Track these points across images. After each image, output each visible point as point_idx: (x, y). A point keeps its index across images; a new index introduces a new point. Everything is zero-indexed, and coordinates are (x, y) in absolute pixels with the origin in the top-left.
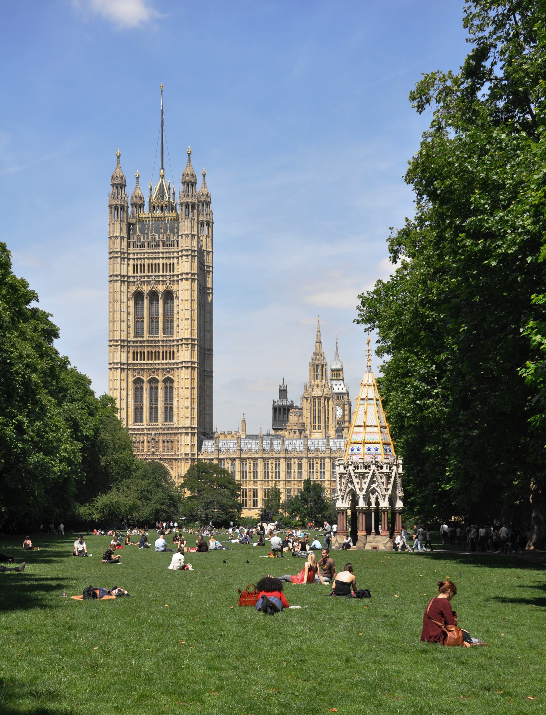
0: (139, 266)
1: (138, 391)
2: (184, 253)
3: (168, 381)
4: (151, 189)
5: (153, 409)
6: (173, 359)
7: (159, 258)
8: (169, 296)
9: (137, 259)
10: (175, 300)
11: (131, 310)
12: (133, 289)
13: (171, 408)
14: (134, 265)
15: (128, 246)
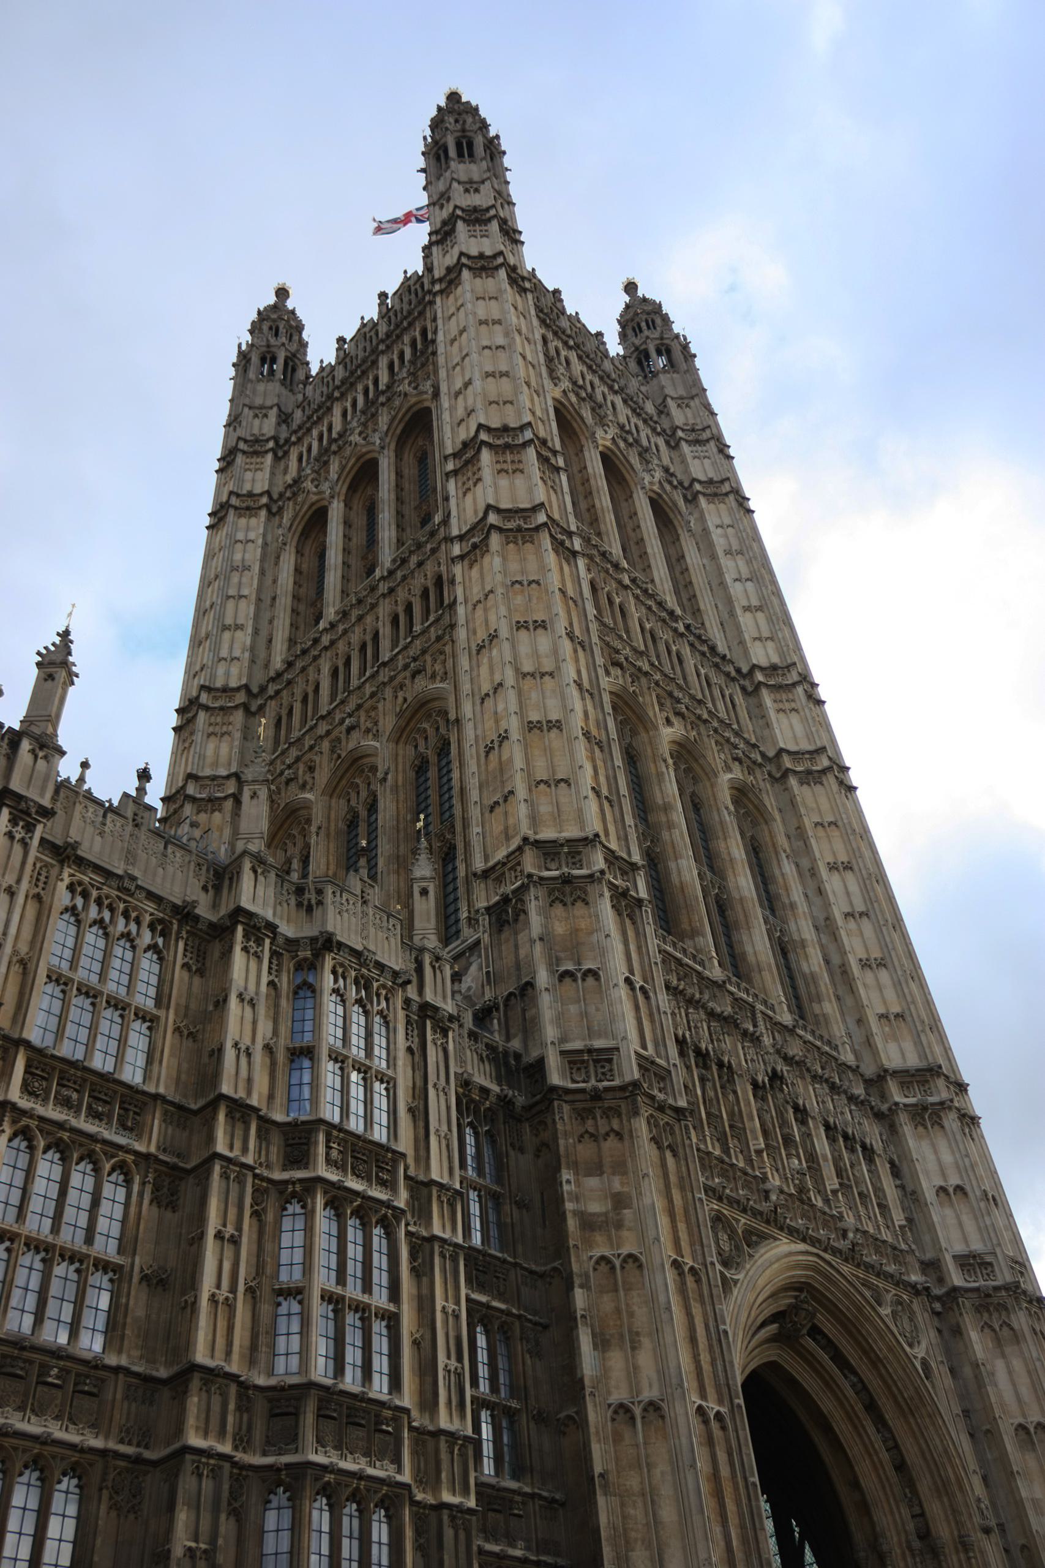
7: (375, 363)
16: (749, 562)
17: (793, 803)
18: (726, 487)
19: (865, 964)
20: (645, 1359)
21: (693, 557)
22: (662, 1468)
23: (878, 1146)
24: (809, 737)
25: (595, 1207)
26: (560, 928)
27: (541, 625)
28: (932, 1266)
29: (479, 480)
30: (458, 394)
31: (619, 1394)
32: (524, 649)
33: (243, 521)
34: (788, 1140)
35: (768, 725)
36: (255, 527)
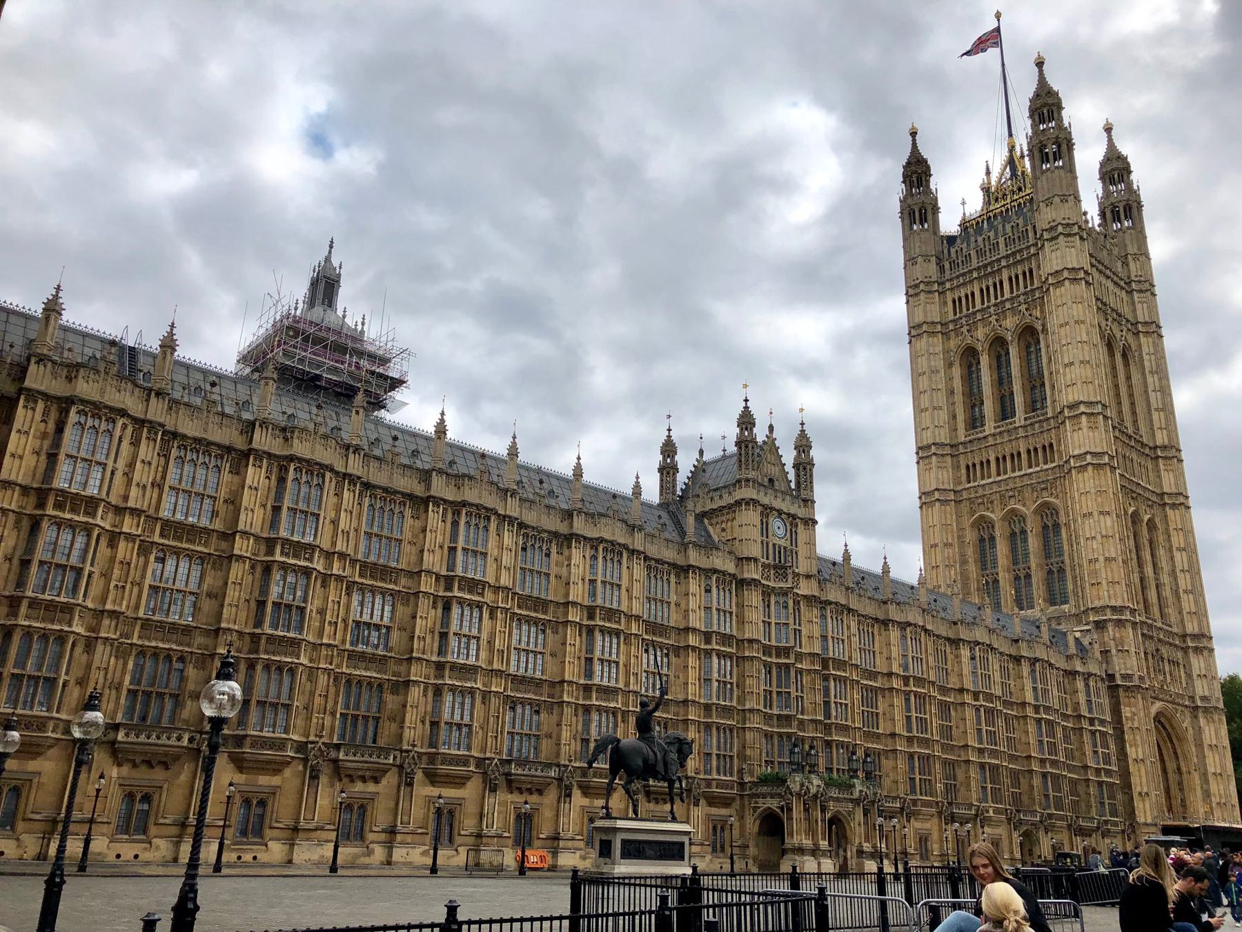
0: (964, 300)
1: (985, 544)
2: (1046, 235)
3: (1046, 510)
4: (988, 173)
5: (1022, 580)
6: (1053, 461)
7: (999, 270)
8: (1030, 335)
9: (958, 286)
10: (1041, 337)
11: (957, 384)
12: (953, 344)
13: (1061, 571)
14: (954, 301)
15: (942, 269)
16: (1160, 379)
17: (1166, 516)
18: (1153, 328)
19: (1185, 591)
20: (1140, 750)
21: (1136, 378)
22: (1143, 770)
23: (1181, 661)
24: (1176, 484)
25: (1129, 715)
26: (1117, 635)
27: (1108, 513)
28: (1192, 698)
29: (1080, 429)
30: (1066, 366)
31: (1134, 756)
32: (1103, 525)
33: (931, 339)
34: (1160, 670)
35: (1159, 477)
36: (937, 343)
